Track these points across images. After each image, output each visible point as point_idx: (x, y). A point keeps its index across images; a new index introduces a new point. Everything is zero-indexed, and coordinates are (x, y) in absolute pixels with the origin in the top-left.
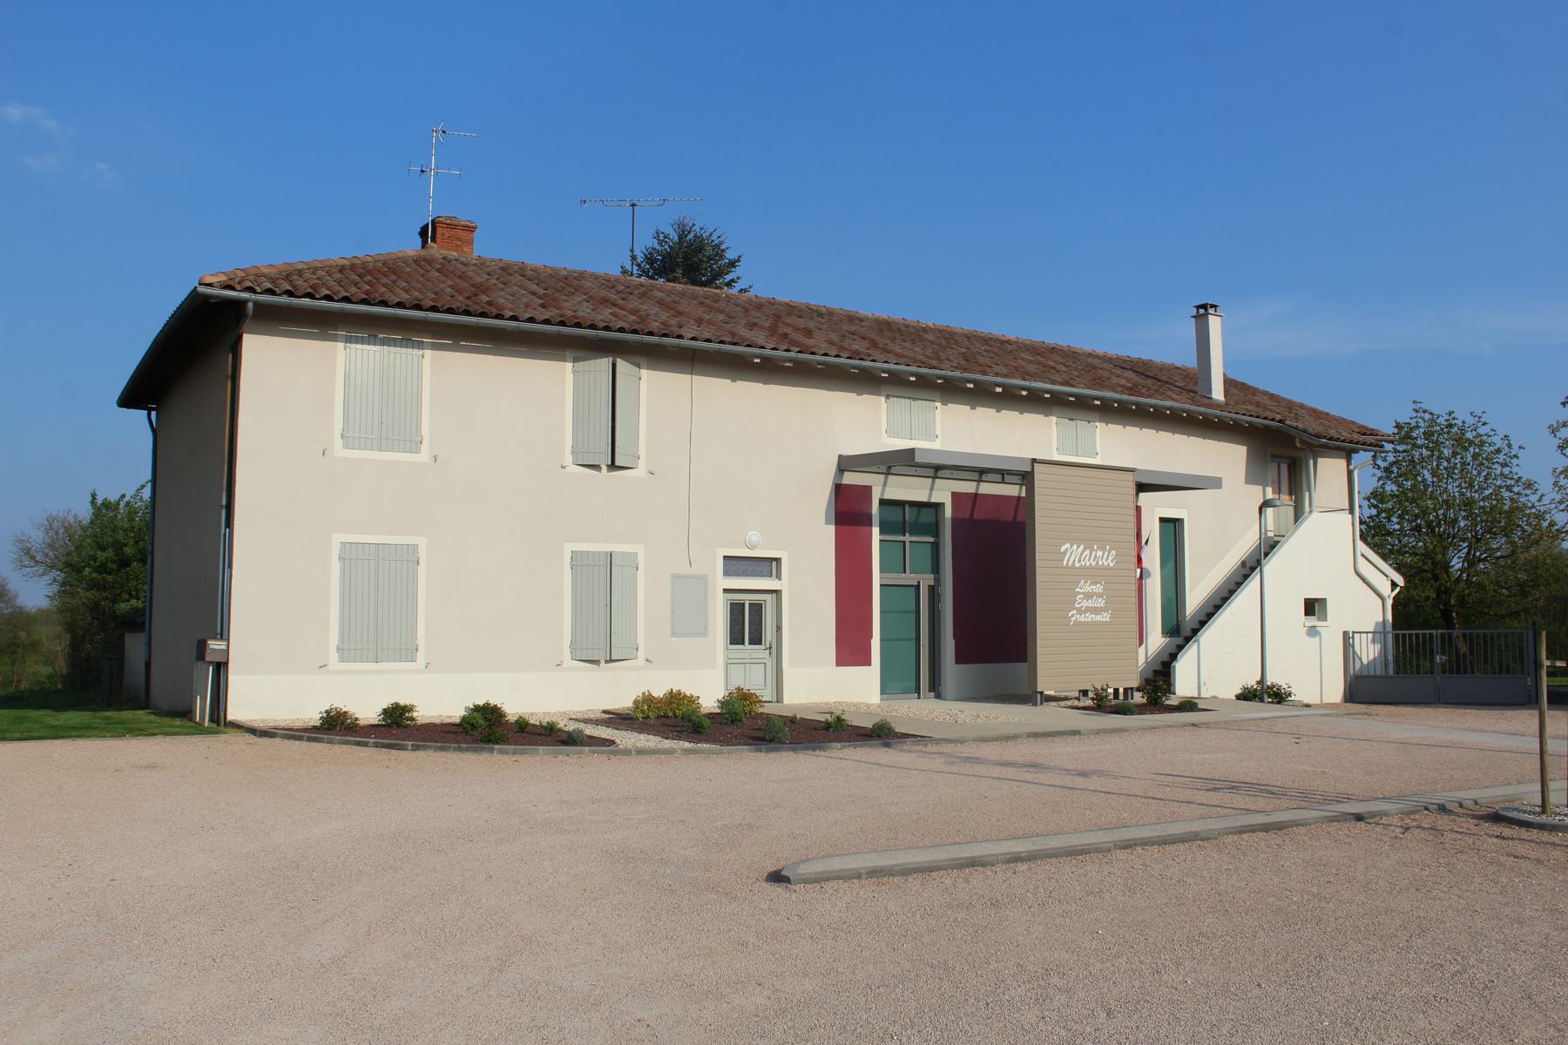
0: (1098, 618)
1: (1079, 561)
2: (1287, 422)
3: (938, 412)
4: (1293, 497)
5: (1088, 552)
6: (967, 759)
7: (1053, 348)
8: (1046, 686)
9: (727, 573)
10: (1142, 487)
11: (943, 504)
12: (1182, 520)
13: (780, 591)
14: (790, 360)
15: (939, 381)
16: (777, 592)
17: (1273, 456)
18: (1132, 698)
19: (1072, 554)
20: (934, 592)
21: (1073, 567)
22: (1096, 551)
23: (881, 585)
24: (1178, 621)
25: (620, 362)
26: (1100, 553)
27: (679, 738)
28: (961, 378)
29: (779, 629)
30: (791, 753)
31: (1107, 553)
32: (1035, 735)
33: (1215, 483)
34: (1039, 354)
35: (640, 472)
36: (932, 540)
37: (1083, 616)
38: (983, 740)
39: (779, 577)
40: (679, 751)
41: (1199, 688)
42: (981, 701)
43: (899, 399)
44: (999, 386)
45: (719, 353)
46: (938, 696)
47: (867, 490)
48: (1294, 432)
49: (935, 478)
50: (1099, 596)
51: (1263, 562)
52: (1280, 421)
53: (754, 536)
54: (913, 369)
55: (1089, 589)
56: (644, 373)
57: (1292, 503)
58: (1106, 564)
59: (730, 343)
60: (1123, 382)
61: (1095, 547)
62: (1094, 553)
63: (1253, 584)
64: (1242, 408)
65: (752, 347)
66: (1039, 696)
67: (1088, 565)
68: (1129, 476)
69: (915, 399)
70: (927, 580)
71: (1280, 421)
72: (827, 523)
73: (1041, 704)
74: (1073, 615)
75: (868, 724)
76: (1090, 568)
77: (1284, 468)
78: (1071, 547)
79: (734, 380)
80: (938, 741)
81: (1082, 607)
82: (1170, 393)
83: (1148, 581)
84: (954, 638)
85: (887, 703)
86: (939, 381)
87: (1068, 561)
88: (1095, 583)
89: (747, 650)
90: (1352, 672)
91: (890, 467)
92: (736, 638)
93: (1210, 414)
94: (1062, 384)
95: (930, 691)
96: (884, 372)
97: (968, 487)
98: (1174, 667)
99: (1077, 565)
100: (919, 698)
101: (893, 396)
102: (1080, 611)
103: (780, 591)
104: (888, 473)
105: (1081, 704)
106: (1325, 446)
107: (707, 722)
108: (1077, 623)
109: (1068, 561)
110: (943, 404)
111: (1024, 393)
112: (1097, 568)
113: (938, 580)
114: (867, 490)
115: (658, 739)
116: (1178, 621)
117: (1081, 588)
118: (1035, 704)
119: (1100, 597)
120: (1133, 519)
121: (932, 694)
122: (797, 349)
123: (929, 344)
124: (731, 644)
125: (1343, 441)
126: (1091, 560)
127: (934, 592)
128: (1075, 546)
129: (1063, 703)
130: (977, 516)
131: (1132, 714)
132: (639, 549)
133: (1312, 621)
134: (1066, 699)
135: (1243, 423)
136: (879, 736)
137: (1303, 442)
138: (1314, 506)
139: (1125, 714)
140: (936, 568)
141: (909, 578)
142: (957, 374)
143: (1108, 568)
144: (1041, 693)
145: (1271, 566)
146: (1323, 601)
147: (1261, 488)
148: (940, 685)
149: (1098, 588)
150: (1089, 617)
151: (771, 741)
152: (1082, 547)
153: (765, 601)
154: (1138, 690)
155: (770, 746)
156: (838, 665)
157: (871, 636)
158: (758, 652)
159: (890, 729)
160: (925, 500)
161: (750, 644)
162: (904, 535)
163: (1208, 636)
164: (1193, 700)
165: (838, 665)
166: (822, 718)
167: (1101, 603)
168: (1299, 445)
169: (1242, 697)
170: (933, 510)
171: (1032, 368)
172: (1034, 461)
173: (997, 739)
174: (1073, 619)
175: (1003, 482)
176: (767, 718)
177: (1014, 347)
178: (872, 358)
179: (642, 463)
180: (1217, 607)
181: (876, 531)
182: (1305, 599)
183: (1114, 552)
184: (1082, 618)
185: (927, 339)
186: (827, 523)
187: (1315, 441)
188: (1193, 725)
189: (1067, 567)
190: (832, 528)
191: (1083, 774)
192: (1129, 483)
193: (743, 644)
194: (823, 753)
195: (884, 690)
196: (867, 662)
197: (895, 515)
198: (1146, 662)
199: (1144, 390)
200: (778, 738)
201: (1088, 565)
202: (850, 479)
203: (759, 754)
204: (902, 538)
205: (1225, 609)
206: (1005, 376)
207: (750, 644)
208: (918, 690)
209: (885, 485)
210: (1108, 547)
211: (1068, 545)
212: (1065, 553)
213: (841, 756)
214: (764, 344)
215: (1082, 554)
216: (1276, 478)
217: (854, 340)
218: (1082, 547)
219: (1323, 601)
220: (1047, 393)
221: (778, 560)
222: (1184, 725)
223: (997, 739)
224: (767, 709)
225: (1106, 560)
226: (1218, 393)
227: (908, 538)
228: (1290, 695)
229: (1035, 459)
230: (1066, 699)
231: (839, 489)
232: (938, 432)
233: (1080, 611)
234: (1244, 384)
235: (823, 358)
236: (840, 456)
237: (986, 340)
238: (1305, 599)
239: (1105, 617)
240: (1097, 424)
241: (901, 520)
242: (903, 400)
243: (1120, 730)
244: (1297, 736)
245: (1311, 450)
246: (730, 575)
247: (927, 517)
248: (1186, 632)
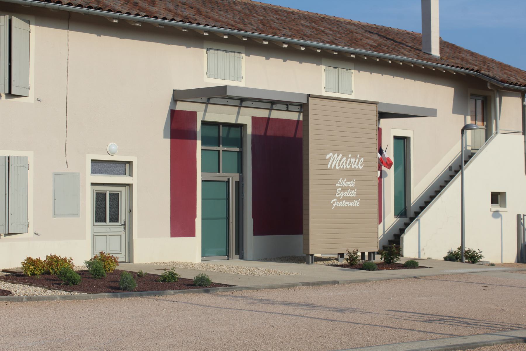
0: (351, 204)
1: (339, 165)
2: (482, 72)
3: (243, 61)
4: (485, 123)
5: (345, 159)
6: (261, 301)
7: (323, 18)
8: (315, 250)
9: (94, 172)
10: (382, 115)
11: (246, 125)
12: (409, 138)
13: (132, 184)
14: (139, 22)
15: (244, 39)
16: (130, 186)
17: (472, 95)
18: (374, 259)
19: (334, 160)
20: (239, 185)
21: (335, 169)
23: (202, 181)
24: (405, 207)
25: (16, 21)
26: (353, 160)
27: (58, 288)
28: (260, 37)
29: (131, 211)
30: (138, 298)
31: (357, 160)
32: (308, 284)
33: (431, 113)
34: (314, 22)
35: (30, 99)
36: (238, 149)
37: (341, 202)
38: (272, 287)
39: (131, 175)
40: (58, 298)
41: (419, 252)
42: (271, 261)
43: (216, 52)
44: (285, 43)
45: (87, 15)
46: (242, 258)
47: (193, 115)
48: (486, 79)
49: (240, 106)
50: (352, 189)
51: (464, 167)
52: (477, 71)
53: (113, 146)
54: (226, 30)
55: (345, 184)
56: (33, 27)
57: (484, 127)
58: (357, 167)
59: (96, 8)
60: (371, 42)
61: (350, 156)
62: (349, 159)
63: (456, 183)
64: (451, 61)
65: (112, 11)
66: (310, 257)
67: (344, 168)
68: (374, 107)
69: (227, 51)
70: (234, 177)
71: (477, 71)
72: (165, 137)
73: (312, 263)
74: (334, 202)
75: (191, 276)
76: (347, 170)
77: (479, 103)
78: (334, 155)
79: (99, 35)
80: (241, 289)
81: (340, 196)
82: (403, 50)
83: (385, 179)
84: (253, 218)
85: (206, 262)
86: (244, 39)
87: (331, 165)
89: (108, 226)
90: (522, 242)
91: (209, 99)
92: (100, 217)
93: (430, 66)
94: (329, 43)
95: (236, 254)
96: (206, 32)
97: (263, 114)
98: (403, 238)
99: (337, 168)
100: (228, 259)
101: (212, 49)
102: (339, 199)
103: (132, 184)
104: (208, 103)
105: (339, 263)
106: (508, 89)
107: (79, 277)
108: (337, 208)
109: (331, 165)
110: (246, 55)
111: (303, 49)
112: (351, 170)
113: (242, 178)
114: (193, 115)
115: (43, 289)
116: (405, 207)
117: (340, 184)
118: (308, 263)
119: (352, 190)
120: (376, 137)
121: (237, 256)
122: (145, 14)
123: (237, 13)
124: (96, 222)
125: (520, 85)
126: (347, 164)
127: (239, 185)
128: (336, 155)
129: (327, 262)
130: (270, 133)
131: (374, 270)
132: (30, 155)
133: (496, 207)
134: (329, 259)
135: (452, 72)
136: (200, 286)
137: (492, 85)
138: (499, 129)
139: (369, 270)
140: (241, 170)
141: (222, 176)
142: (257, 34)
143: (358, 170)
144: (312, 255)
145: (469, 170)
146: (503, 194)
147: (463, 116)
148: (243, 250)
149: (352, 184)
151: (125, 289)
152: (341, 155)
153: (121, 191)
154: (378, 253)
155: (123, 293)
156: (172, 236)
157: (195, 216)
158: (115, 227)
159: (208, 280)
160: (233, 121)
161: (110, 221)
162: (219, 146)
163: (426, 217)
164: (415, 261)
165: (172, 236)
166: (160, 273)
167: (353, 194)
168: (489, 87)
169: (448, 259)
170: (239, 129)
171: (308, 32)
172: (309, 96)
173: (282, 287)
174: (334, 205)
175: (287, 110)
176: (120, 273)
177: (296, 16)
178: (197, 22)
179: (32, 93)
180: (432, 198)
181: (199, 143)
182: (492, 193)
183: (362, 159)
184: (341, 204)
185: (236, 10)
186: (165, 137)
187: (500, 85)
188: (415, 277)
189: (330, 169)
190: (168, 141)
191: (340, 311)
192: (373, 112)
193: (105, 221)
194: (161, 297)
195: (203, 255)
196: (192, 234)
197: (212, 132)
198: (384, 234)
199: (385, 48)
200: (129, 287)
201: (344, 168)
202: (181, 106)
203: (115, 299)
204: (217, 148)
205: (437, 199)
206: (290, 36)
207: (110, 221)
208: (227, 254)
209: (205, 111)
210: (358, 157)
211: (331, 154)
212: (329, 159)
213: (174, 299)
214: (120, 10)
215: (340, 160)
216: (474, 110)
217: (185, 9)
218: (341, 155)
219: (503, 194)
220: (319, 48)
221: (130, 163)
222: (409, 278)
223: (282, 287)
224: (120, 267)
225: (357, 165)
226: (435, 51)
227: (221, 148)
228: (480, 257)
229: (310, 95)
230: (329, 259)
231: (173, 114)
232: (243, 75)
233: (339, 199)
234: (453, 45)
235: (163, 21)
236: (174, 90)
237: (277, 11)
238: (492, 193)
239: (356, 204)
240: (353, 71)
241: (217, 135)
242: (219, 52)
243: (365, 281)
244: (485, 285)
245: (498, 91)
246: (96, 173)
247: (234, 133)
248: (411, 214)
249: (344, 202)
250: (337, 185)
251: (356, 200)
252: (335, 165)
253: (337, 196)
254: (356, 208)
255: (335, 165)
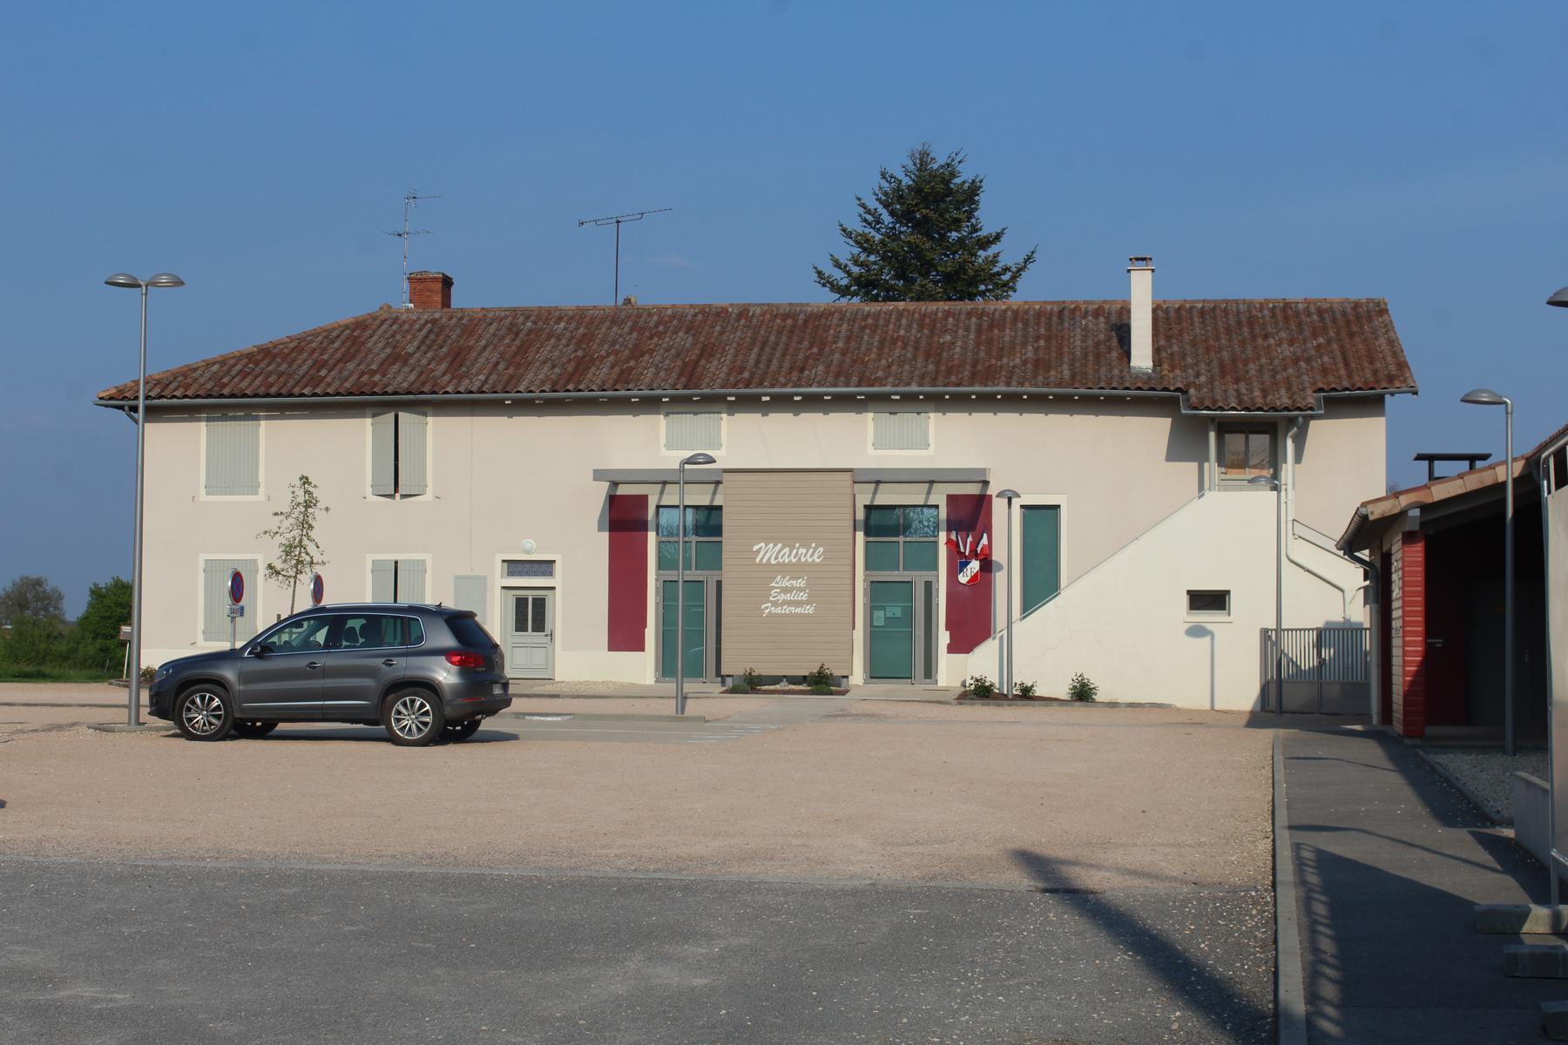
0: (798, 610)
1: (776, 558)
21: (768, 563)
22: (798, 549)
31: (811, 550)
50: (800, 589)
61: (797, 545)
74: (767, 608)
76: (790, 563)
81: (778, 600)
87: (762, 558)
88: (797, 578)
99: (773, 562)
102: (775, 604)
109: (762, 558)
110: (729, 415)
119: (801, 592)
126: (792, 557)
143: (813, 564)
149: (801, 583)
150: (787, 610)
152: (780, 545)
167: (803, 596)
174: (767, 611)
183: (821, 549)
184: (779, 610)
189: (761, 564)
210: (813, 545)
211: (763, 544)
212: (759, 551)
215: (779, 552)
218: (780, 545)
225: (811, 556)
233: (775, 604)
240: (932, 415)
249: (784, 607)
250: (773, 584)
251: (807, 604)
252: (770, 558)
253: (771, 598)
254: (809, 615)
255: (770, 558)
